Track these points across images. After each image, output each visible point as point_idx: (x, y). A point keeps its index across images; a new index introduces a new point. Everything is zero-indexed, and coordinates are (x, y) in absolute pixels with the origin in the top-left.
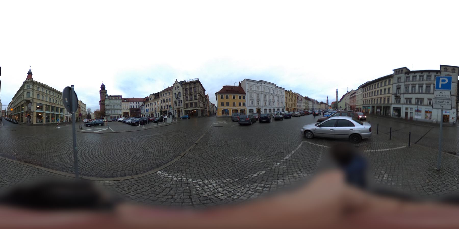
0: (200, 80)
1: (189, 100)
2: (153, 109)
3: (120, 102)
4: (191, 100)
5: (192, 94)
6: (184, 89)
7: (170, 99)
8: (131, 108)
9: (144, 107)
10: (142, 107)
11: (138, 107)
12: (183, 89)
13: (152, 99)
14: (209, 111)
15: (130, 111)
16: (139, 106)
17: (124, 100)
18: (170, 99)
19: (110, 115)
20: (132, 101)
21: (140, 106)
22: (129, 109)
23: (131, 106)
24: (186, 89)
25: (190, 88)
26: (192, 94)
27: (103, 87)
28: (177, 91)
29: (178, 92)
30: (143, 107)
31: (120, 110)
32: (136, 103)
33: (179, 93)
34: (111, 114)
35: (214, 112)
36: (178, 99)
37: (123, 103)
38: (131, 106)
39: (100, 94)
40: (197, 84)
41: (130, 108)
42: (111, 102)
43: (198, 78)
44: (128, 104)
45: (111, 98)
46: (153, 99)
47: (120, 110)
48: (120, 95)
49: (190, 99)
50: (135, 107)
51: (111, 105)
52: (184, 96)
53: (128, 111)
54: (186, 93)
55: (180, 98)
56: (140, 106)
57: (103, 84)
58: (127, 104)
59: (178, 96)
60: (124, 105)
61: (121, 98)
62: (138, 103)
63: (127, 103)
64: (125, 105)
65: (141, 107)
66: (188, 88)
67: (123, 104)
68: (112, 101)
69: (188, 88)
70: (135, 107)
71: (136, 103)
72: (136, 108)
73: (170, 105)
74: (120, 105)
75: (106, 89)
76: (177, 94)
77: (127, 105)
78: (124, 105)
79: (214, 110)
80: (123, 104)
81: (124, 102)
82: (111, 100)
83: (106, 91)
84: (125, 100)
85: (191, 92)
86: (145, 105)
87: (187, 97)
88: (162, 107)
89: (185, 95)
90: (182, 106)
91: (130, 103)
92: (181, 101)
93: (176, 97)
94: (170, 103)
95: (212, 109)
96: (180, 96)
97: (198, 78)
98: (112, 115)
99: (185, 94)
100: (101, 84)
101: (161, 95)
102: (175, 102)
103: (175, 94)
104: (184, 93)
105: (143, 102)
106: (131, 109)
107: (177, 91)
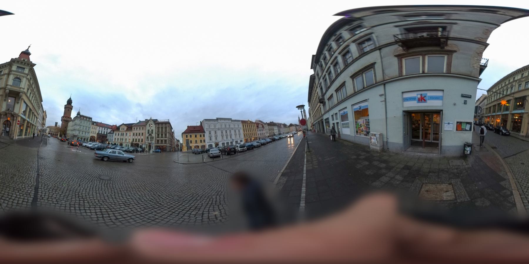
0: (170, 122)
1: (160, 137)
2: (123, 139)
4: (162, 137)
5: (163, 133)
6: (157, 128)
7: (142, 134)
8: (99, 133)
9: (113, 135)
10: (110, 134)
11: (105, 133)
12: (156, 127)
13: (124, 129)
15: (97, 136)
16: (107, 133)
17: (93, 123)
18: (142, 134)
19: (77, 135)
20: (101, 127)
21: (108, 133)
22: (96, 133)
23: (99, 131)
24: (158, 128)
25: (162, 128)
26: (163, 133)
28: (151, 128)
29: (151, 129)
30: (112, 134)
32: (105, 130)
33: (152, 130)
34: (78, 135)
36: (150, 135)
38: (99, 131)
39: (64, 109)
40: (167, 124)
42: (81, 123)
43: (169, 120)
44: (97, 128)
46: (125, 129)
47: (88, 133)
48: (91, 117)
49: (161, 137)
50: (103, 133)
51: (81, 126)
52: (156, 133)
53: (96, 136)
54: (158, 131)
55: (152, 134)
56: (108, 133)
57: (70, 98)
58: (95, 128)
59: (150, 133)
61: (91, 120)
62: (106, 129)
63: (96, 127)
64: (94, 129)
65: (108, 134)
66: (160, 127)
68: (83, 121)
69: (160, 127)
70: (103, 133)
71: (105, 130)
73: (142, 140)
75: (72, 104)
76: (150, 130)
77: (96, 129)
80: (91, 127)
81: (93, 126)
82: (82, 120)
83: (72, 107)
84: (95, 124)
85: (162, 131)
86: (115, 133)
87: (158, 135)
88: (133, 139)
89: (157, 133)
90: (154, 142)
91: (99, 127)
92: (153, 137)
93: (148, 133)
94: (142, 137)
96: (152, 133)
97: (169, 120)
98: (79, 136)
99: (157, 132)
101: (134, 128)
102: (147, 137)
103: (149, 131)
104: (157, 131)
105: (111, 130)
106: (98, 134)
107: (151, 128)
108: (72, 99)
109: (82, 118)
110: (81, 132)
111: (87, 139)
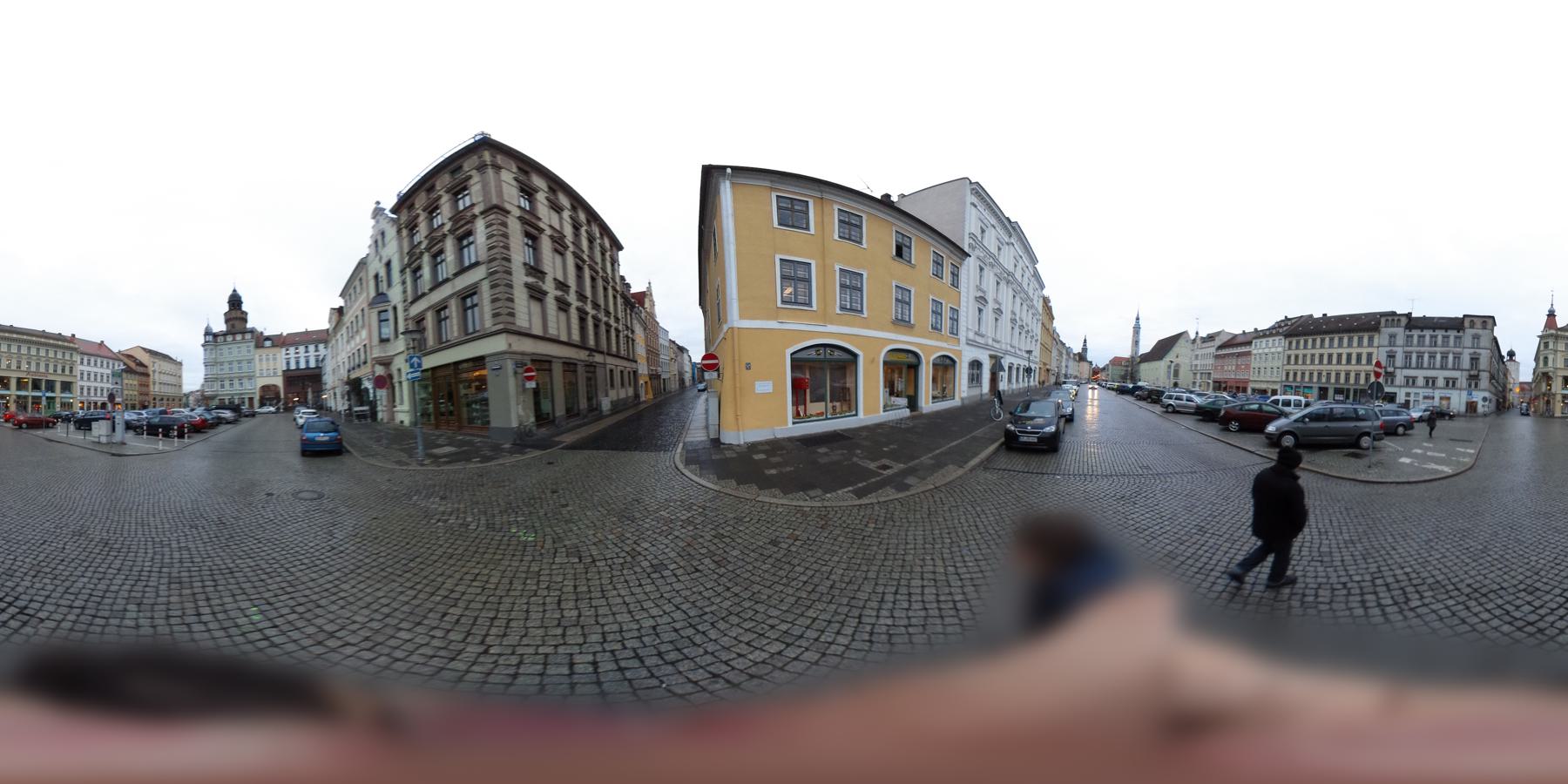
3: (249, 351)
8: (288, 370)
14: (655, 377)
16: (317, 361)
20: (292, 345)
22: (280, 373)
23: (288, 363)
27: (235, 301)
31: (250, 378)
34: (220, 393)
35: (682, 381)
37: (258, 354)
38: (288, 363)
41: (285, 368)
42: (221, 354)
44: (278, 356)
45: (222, 338)
47: (250, 378)
51: (222, 364)
53: (279, 382)
58: (271, 356)
60: (261, 360)
67: (257, 357)
68: (225, 349)
72: (298, 369)
74: (249, 361)
77: (275, 359)
78: (261, 360)
79: (681, 374)
80: (257, 357)
81: (260, 351)
84: (268, 343)
91: (284, 350)
95: (674, 369)
100: (230, 292)
108: (240, 292)
109: (220, 339)
110: (227, 383)
111: (251, 399)
